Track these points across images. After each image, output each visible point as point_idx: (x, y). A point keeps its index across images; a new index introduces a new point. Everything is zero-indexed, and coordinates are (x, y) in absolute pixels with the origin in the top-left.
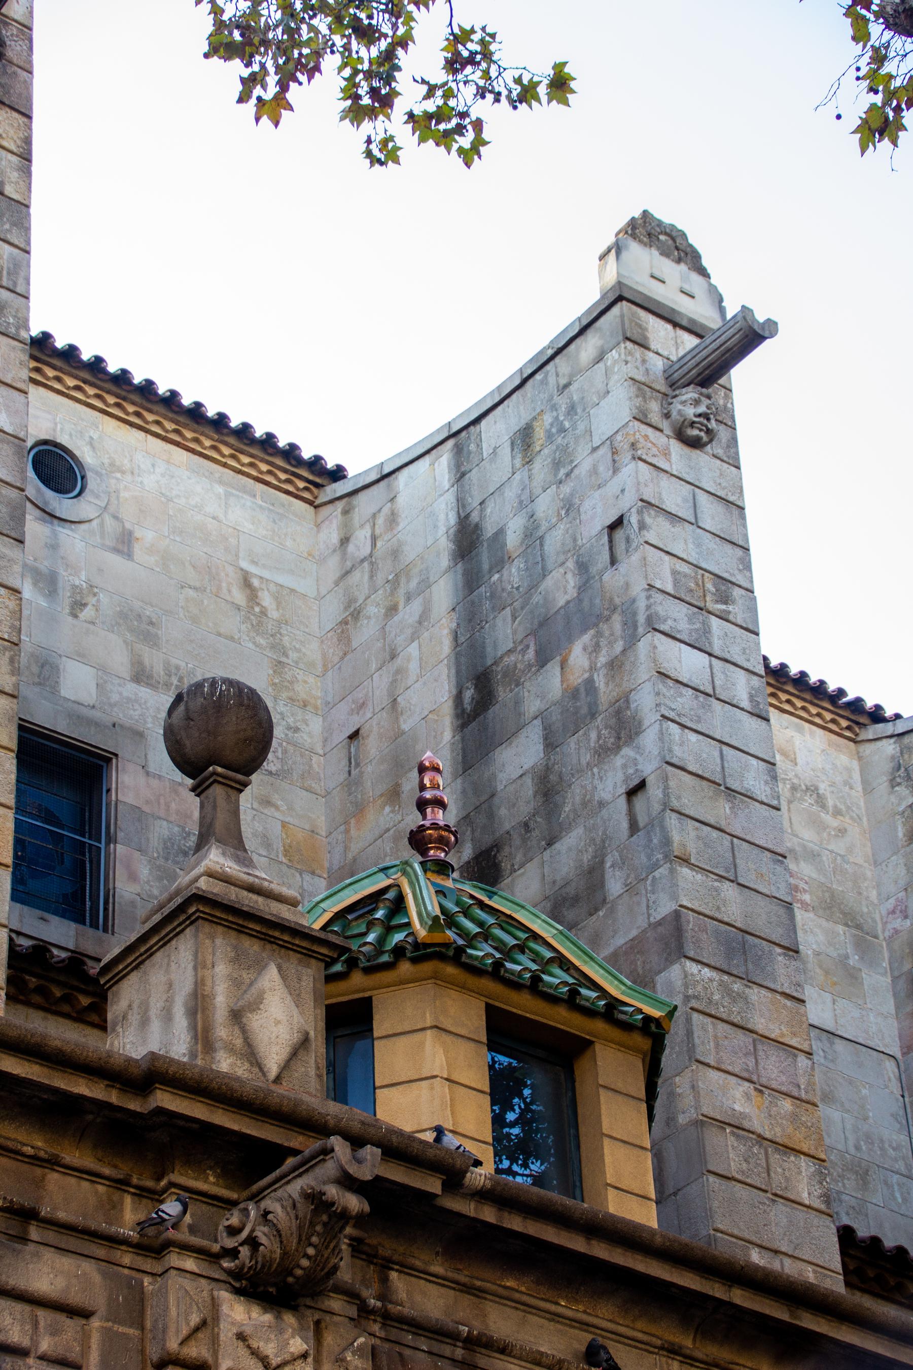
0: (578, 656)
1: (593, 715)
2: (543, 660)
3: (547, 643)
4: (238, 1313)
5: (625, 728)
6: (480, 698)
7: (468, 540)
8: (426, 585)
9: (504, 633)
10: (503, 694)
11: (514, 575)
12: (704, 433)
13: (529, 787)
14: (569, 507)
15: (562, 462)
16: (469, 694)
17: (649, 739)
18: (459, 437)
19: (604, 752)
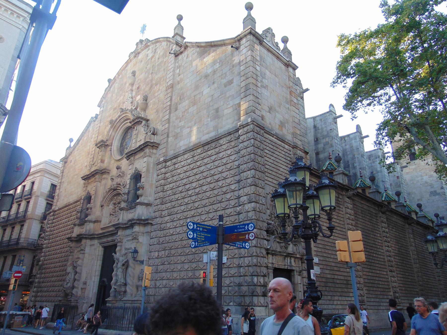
0: (327, 139)
1: (329, 144)
2: (323, 139)
3: (324, 137)
4: (347, 199)
5: (332, 146)
6: (317, 140)
7: (315, 127)
8: (310, 129)
9: (319, 136)
10: (319, 140)
11: (320, 131)
12: (336, 123)
13: (322, 148)
14: (326, 127)
15: (325, 123)
16: (315, 139)
17: (334, 147)
18: (314, 118)
19: (330, 147)
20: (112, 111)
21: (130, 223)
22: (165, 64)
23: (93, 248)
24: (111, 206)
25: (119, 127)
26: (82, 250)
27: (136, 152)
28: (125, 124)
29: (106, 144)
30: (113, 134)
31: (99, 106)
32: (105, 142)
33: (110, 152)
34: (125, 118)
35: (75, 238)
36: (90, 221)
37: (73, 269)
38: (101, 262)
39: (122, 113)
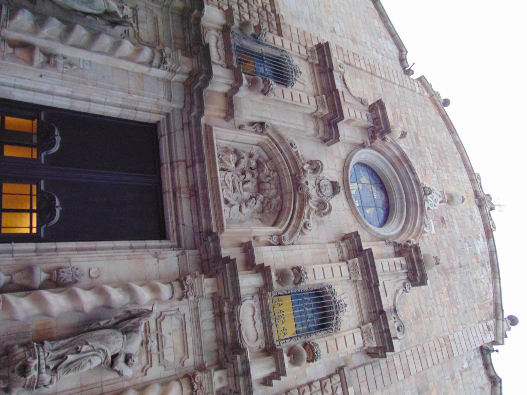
20: (415, 130)
21: (240, 367)
22: (472, 310)
23: (162, 96)
24: (255, 150)
25: (396, 170)
26: (163, 61)
27: (371, 290)
28: (400, 189)
29: (378, 134)
30: (389, 154)
31: (422, 80)
32: (382, 134)
33: (360, 142)
34: (411, 198)
35: (198, 19)
36: (235, 89)
37: (107, 13)
38: (116, 116)
39: (423, 192)
